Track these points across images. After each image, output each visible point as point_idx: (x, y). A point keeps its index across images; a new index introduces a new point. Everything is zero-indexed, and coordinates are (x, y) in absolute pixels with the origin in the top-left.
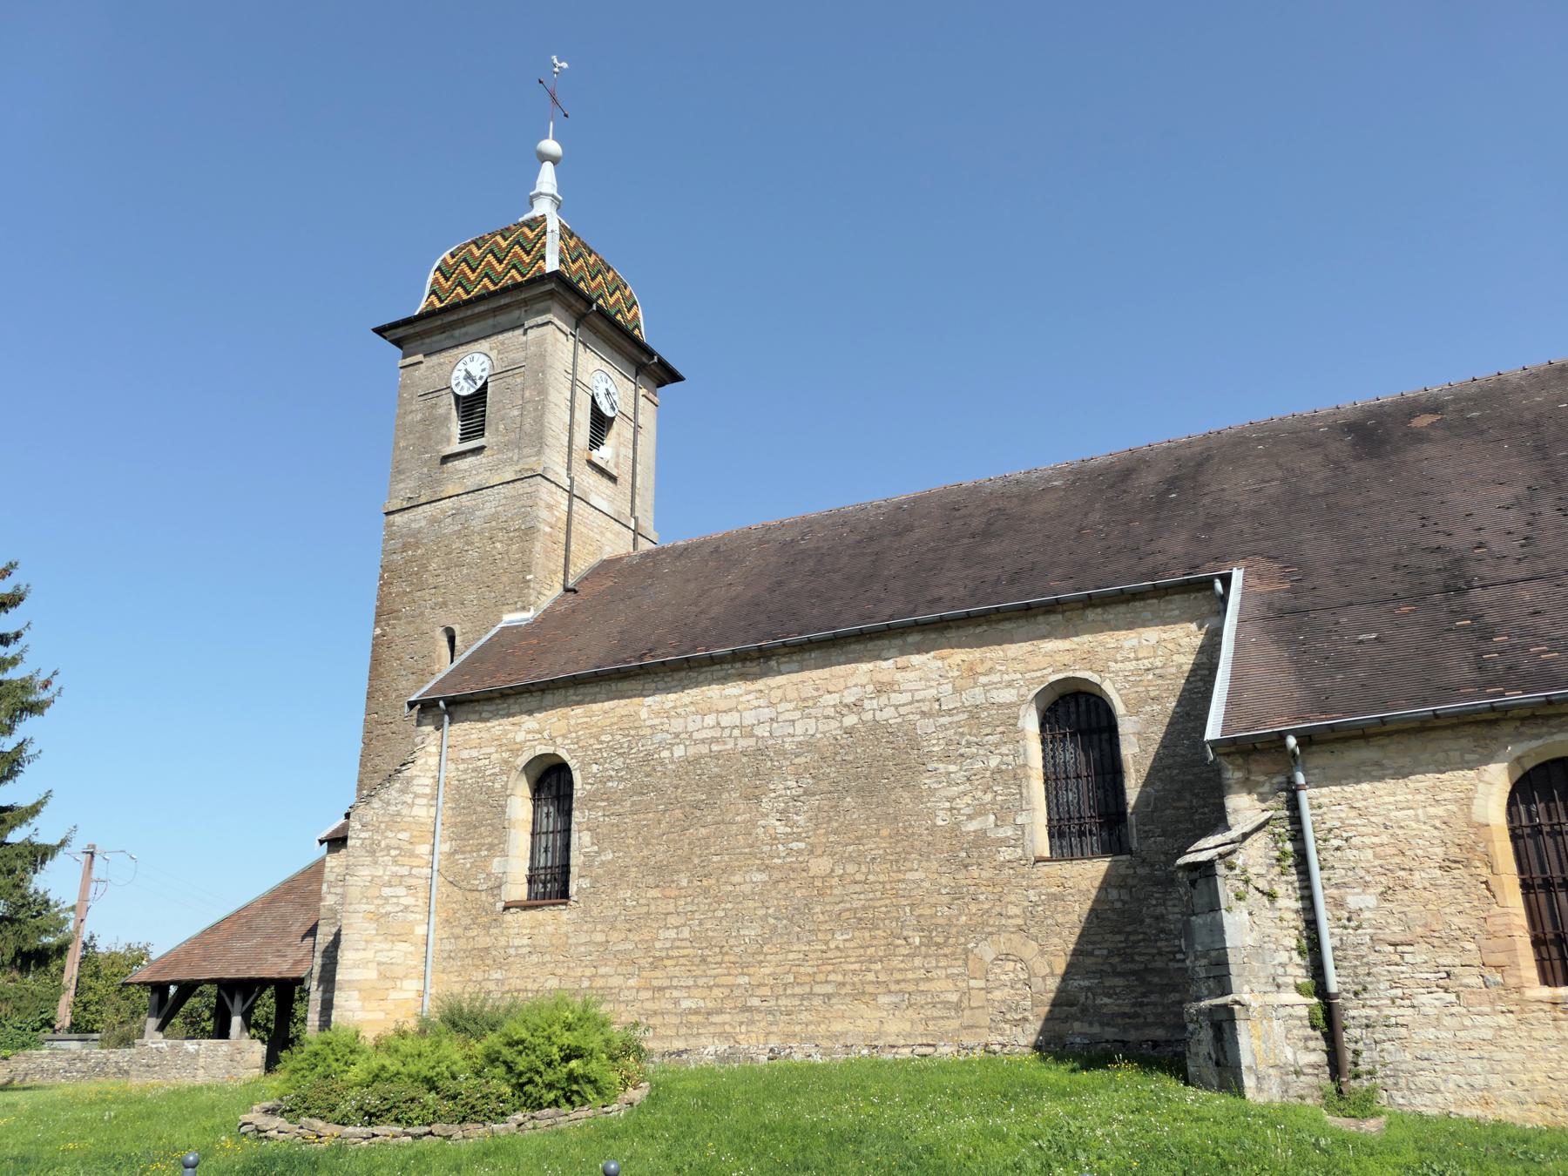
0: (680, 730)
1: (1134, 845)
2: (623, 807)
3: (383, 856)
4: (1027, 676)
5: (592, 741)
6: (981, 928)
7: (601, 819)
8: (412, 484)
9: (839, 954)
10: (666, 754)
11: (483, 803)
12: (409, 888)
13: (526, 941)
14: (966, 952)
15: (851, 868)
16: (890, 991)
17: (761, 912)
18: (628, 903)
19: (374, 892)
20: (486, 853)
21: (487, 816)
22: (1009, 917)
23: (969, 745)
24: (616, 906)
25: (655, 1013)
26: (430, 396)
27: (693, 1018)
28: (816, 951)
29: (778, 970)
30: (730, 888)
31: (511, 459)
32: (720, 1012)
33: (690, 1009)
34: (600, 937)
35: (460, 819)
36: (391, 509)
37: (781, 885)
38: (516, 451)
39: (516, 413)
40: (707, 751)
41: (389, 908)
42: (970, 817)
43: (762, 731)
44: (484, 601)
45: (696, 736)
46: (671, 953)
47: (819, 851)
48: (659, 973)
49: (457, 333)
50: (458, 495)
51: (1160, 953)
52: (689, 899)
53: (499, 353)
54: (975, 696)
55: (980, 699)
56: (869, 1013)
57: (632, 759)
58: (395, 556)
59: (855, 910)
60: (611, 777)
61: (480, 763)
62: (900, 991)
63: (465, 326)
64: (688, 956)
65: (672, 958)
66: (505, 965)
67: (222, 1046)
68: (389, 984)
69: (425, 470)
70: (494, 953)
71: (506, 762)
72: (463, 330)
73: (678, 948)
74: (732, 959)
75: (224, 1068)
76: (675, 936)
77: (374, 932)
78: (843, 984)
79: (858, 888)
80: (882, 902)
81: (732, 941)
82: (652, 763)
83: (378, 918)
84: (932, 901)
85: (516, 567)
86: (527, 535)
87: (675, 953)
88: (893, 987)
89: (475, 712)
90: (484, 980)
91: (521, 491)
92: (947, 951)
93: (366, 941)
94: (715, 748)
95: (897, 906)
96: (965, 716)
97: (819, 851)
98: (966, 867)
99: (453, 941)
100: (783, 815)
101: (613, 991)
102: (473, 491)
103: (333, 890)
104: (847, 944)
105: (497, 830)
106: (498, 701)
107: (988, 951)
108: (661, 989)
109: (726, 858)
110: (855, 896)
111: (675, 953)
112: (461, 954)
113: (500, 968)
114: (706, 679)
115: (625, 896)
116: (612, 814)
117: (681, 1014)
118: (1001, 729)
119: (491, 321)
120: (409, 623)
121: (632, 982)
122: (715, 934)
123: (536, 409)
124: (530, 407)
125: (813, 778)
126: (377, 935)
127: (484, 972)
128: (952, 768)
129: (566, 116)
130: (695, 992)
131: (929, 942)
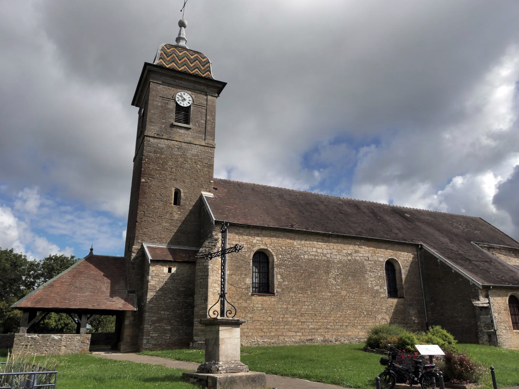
0: (306, 250)
1: (405, 296)
4: (385, 256)
5: (279, 248)
6: (378, 312)
9: (349, 315)
10: (302, 256)
11: (242, 260)
14: (375, 317)
15: (351, 295)
16: (360, 325)
17: (330, 303)
18: (293, 297)
21: (244, 265)
22: (383, 310)
23: (375, 269)
24: (289, 297)
25: (302, 329)
26: (165, 99)
27: (313, 330)
28: (343, 314)
29: (335, 319)
30: (321, 296)
31: (202, 137)
32: (320, 329)
33: (312, 328)
34: (285, 306)
36: (149, 135)
37: (335, 297)
38: (204, 135)
39: (203, 122)
42: (375, 286)
43: (328, 256)
44: (194, 184)
45: (311, 253)
46: (306, 312)
47: (343, 289)
48: (303, 318)
49: (177, 81)
50: (180, 142)
51: (409, 319)
52: (311, 298)
53: (195, 97)
54: (375, 258)
55: (376, 259)
56: (356, 330)
58: (151, 154)
59: (352, 305)
62: (362, 325)
64: (311, 313)
65: (307, 314)
66: (253, 312)
67: (77, 337)
69: (163, 126)
70: (249, 308)
71: (249, 248)
72: (180, 82)
74: (323, 315)
78: (350, 323)
79: (352, 300)
80: (357, 304)
81: (323, 310)
82: (299, 258)
84: (368, 304)
85: (206, 176)
87: (307, 312)
88: (361, 324)
89: (237, 229)
90: (245, 317)
91: (207, 151)
92: (372, 316)
93: (212, 302)
94: (316, 258)
95: (362, 305)
96: (373, 262)
97: (343, 289)
98: (375, 297)
100: (335, 279)
102: (187, 143)
103: (154, 279)
104: (351, 313)
106: (246, 228)
107: (379, 317)
108: (304, 322)
109: (320, 288)
110: (352, 302)
111: (307, 312)
113: (251, 313)
117: (309, 329)
118: (380, 267)
119: (192, 84)
120: (159, 182)
121: (295, 320)
122: (318, 308)
124: (209, 123)
125: (342, 270)
126: (214, 300)
127: (245, 314)
128: (372, 274)
129: (181, 11)
130: (313, 323)
131: (368, 314)
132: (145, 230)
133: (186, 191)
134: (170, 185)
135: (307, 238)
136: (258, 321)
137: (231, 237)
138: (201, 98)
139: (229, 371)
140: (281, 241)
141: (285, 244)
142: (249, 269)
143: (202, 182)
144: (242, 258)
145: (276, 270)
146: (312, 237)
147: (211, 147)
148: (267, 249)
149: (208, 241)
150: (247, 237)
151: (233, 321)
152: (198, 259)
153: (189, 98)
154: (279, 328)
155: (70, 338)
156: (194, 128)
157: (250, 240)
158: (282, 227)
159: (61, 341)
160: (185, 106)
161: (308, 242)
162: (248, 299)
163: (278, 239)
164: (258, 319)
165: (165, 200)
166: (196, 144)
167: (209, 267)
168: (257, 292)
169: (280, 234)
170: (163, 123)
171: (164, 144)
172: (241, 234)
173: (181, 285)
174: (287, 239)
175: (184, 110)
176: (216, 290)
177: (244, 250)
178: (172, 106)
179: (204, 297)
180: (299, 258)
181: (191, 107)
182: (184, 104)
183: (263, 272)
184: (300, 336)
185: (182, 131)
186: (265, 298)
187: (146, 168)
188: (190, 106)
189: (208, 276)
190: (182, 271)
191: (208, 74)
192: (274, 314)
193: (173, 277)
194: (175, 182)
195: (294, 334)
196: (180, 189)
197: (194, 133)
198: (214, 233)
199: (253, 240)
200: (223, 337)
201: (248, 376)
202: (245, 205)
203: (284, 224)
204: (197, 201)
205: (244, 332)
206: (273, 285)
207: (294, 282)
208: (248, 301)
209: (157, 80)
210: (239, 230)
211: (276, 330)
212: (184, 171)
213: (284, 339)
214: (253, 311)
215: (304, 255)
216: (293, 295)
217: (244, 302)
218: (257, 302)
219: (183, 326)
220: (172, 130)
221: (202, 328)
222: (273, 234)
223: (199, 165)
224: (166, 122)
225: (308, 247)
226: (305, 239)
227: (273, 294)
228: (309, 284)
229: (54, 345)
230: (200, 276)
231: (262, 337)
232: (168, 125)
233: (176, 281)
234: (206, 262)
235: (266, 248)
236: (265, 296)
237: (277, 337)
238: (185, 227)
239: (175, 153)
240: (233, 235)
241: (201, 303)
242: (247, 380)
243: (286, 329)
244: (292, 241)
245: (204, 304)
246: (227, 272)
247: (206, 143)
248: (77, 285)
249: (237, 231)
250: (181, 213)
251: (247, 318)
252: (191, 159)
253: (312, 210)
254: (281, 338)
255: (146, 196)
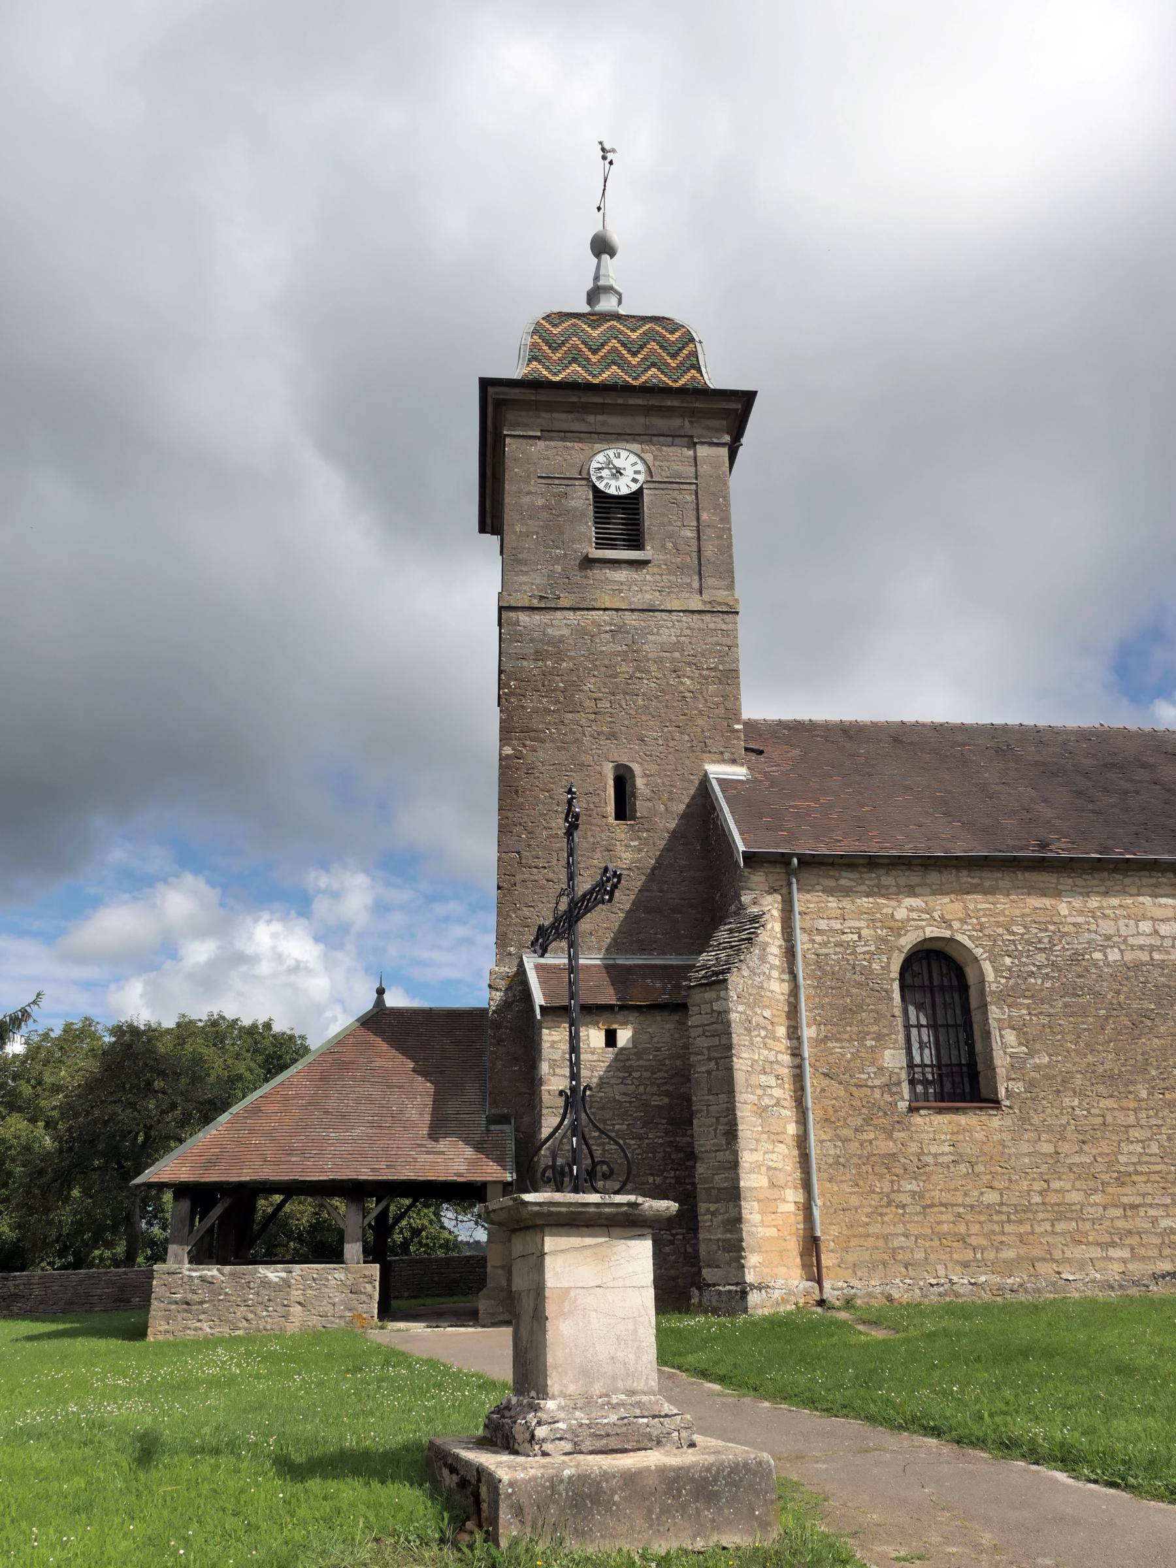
0: (1112, 932)
2: (1052, 1006)
3: (756, 1037)
5: (1000, 931)
7: (1028, 1018)
8: (539, 580)
10: (1098, 955)
11: (859, 985)
12: (777, 1077)
13: (947, 1149)
18: (1077, 1112)
19: (754, 1080)
20: (874, 1043)
24: (1062, 1114)
25: (1130, 1232)
26: (557, 481)
31: (689, 585)
34: (1048, 1148)
35: (827, 1000)
36: (513, 604)
38: (696, 577)
39: (690, 534)
40: (1148, 959)
41: (766, 1101)
44: (675, 743)
45: (1131, 940)
46: (1139, 1168)
48: (1128, 1190)
49: (591, 418)
50: (617, 610)
52: (1151, 1113)
53: (655, 458)
57: (1057, 956)
58: (525, 663)
60: (1033, 973)
61: (844, 937)
63: (603, 414)
65: (1142, 1173)
66: (921, 1175)
67: (334, 1274)
68: (775, 1194)
69: (558, 568)
70: (903, 1160)
71: (884, 940)
72: (600, 418)
73: (1146, 1163)
75: (342, 1302)
76: (1142, 1151)
77: (760, 1129)
82: (1084, 963)
83: (762, 1111)
85: (717, 711)
86: (728, 678)
89: (831, 877)
90: (893, 1192)
91: (712, 626)
93: (757, 1140)
94: (1156, 956)
99: (840, 1144)
101: (1074, 1208)
105: (885, 1017)
106: (863, 870)
112: (855, 1160)
113: (916, 1178)
114: (1133, 883)
115: (1073, 1104)
116: (1041, 1013)
117: (1160, 1234)
119: (641, 420)
120: (559, 749)
121: (1097, 1198)
123: (720, 537)
124: (708, 533)
126: (763, 1132)
127: (892, 1182)
129: (599, 209)
132: (526, 912)
133: (653, 768)
134: (596, 757)
135: (1108, 883)
136: (945, 1205)
137: (812, 906)
138: (675, 458)
139: (587, 1445)
140: (1002, 903)
141: (1023, 916)
142: (889, 1015)
143: (703, 731)
144: (857, 977)
145: (994, 1012)
146: (1128, 881)
147: (723, 612)
148: (951, 940)
149: (727, 927)
150: (871, 900)
151: (607, 1210)
152: (693, 991)
153: (633, 465)
154: (1033, 1233)
155: (315, 1276)
156: (662, 557)
157: (884, 911)
158: (1000, 851)
159: (289, 1287)
160: (624, 491)
161: (1115, 901)
162: (897, 1126)
163: (991, 898)
164: (945, 1197)
165: (585, 805)
166: (670, 611)
167: (733, 1016)
168: (932, 1098)
169: (997, 880)
170: (557, 560)
171: (566, 624)
172: (847, 892)
173: (655, 1088)
174: (1029, 894)
175: (623, 509)
176: (771, 1096)
177: (865, 949)
178: (582, 499)
179: (726, 1124)
180: (1084, 963)
181: (645, 491)
182: (618, 488)
183: (947, 1026)
184: (1124, 1261)
185: (622, 575)
186: (962, 1119)
187: (513, 710)
188: (641, 489)
189: (729, 1047)
190: (655, 1040)
191: (693, 378)
192: (1006, 1177)
193: (623, 1063)
194: (610, 745)
195: (1097, 1252)
196: (631, 765)
197: (661, 575)
198: (746, 898)
199: (894, 908)
200: (565, 1285)
201: (672, 1469)
202: (862, 794)
203: (1012, 843)
204: (693, 798)
205: (894, 1249)
206: (991, 1067)
207: (1073, 1054)
208: (896, 1135)
209: (526, 426)
210: (837, 880)
211: (1021, 1237)
212: (640, 702)
213: (1059, 1273)
214: (920, 1170)
215: (1103, 949)
216: (1076, 1103)
217: (883, 1136)
218: (931, 1136)
219: (674, 1231)
220: (587, 577)
221: (728, 1236)
222: (969, 880)
223: (688, 677)
224: (565, 554)
225: (1116, 919)
226: (1103, 889)
227: (995, 1103)
228: (1139, 1057)
229: (269, 1300)
230: (706, 1052)
231: (966, 1265)
232: (572, 562)
233: (635, 1074)
234: (719, 998)
235: (947, 934)
236: (963, 1110)
237: (1025, 1265)
238: (661, 891)
239: (604, 649)
240: (816, 899)
241: (714, 1145)
242: (668, 1492)
243: (1063, 1234)
244: (1047, 902)
245: (725, 1150)
246: (808, 1033)
247: (704, 603)
248: (331, 1104)
249: (832, 883)
250: (640, 844)
251: (900, 1194)
252: (659, 661)
253: (1129, 786)
254: (1044, 1269)
255: (522, 800)
